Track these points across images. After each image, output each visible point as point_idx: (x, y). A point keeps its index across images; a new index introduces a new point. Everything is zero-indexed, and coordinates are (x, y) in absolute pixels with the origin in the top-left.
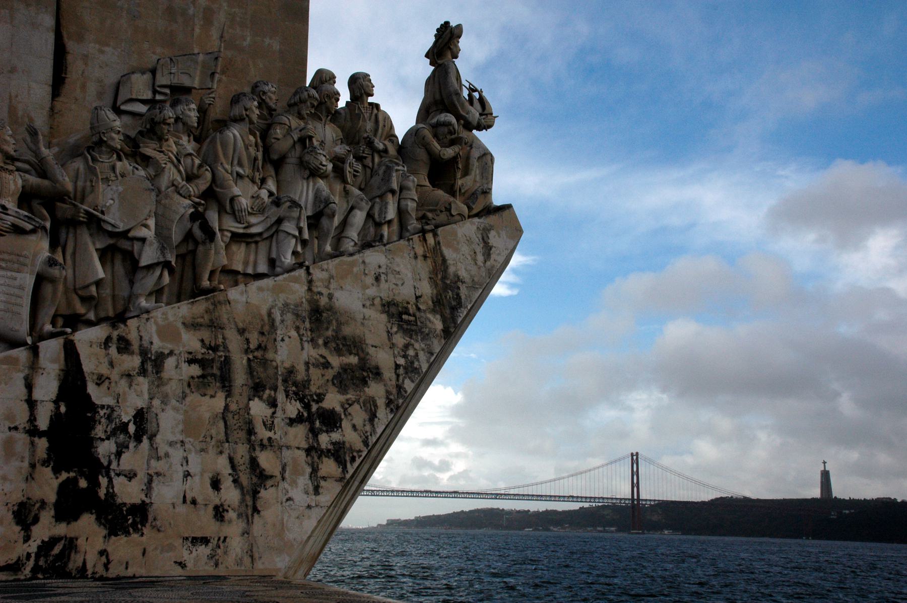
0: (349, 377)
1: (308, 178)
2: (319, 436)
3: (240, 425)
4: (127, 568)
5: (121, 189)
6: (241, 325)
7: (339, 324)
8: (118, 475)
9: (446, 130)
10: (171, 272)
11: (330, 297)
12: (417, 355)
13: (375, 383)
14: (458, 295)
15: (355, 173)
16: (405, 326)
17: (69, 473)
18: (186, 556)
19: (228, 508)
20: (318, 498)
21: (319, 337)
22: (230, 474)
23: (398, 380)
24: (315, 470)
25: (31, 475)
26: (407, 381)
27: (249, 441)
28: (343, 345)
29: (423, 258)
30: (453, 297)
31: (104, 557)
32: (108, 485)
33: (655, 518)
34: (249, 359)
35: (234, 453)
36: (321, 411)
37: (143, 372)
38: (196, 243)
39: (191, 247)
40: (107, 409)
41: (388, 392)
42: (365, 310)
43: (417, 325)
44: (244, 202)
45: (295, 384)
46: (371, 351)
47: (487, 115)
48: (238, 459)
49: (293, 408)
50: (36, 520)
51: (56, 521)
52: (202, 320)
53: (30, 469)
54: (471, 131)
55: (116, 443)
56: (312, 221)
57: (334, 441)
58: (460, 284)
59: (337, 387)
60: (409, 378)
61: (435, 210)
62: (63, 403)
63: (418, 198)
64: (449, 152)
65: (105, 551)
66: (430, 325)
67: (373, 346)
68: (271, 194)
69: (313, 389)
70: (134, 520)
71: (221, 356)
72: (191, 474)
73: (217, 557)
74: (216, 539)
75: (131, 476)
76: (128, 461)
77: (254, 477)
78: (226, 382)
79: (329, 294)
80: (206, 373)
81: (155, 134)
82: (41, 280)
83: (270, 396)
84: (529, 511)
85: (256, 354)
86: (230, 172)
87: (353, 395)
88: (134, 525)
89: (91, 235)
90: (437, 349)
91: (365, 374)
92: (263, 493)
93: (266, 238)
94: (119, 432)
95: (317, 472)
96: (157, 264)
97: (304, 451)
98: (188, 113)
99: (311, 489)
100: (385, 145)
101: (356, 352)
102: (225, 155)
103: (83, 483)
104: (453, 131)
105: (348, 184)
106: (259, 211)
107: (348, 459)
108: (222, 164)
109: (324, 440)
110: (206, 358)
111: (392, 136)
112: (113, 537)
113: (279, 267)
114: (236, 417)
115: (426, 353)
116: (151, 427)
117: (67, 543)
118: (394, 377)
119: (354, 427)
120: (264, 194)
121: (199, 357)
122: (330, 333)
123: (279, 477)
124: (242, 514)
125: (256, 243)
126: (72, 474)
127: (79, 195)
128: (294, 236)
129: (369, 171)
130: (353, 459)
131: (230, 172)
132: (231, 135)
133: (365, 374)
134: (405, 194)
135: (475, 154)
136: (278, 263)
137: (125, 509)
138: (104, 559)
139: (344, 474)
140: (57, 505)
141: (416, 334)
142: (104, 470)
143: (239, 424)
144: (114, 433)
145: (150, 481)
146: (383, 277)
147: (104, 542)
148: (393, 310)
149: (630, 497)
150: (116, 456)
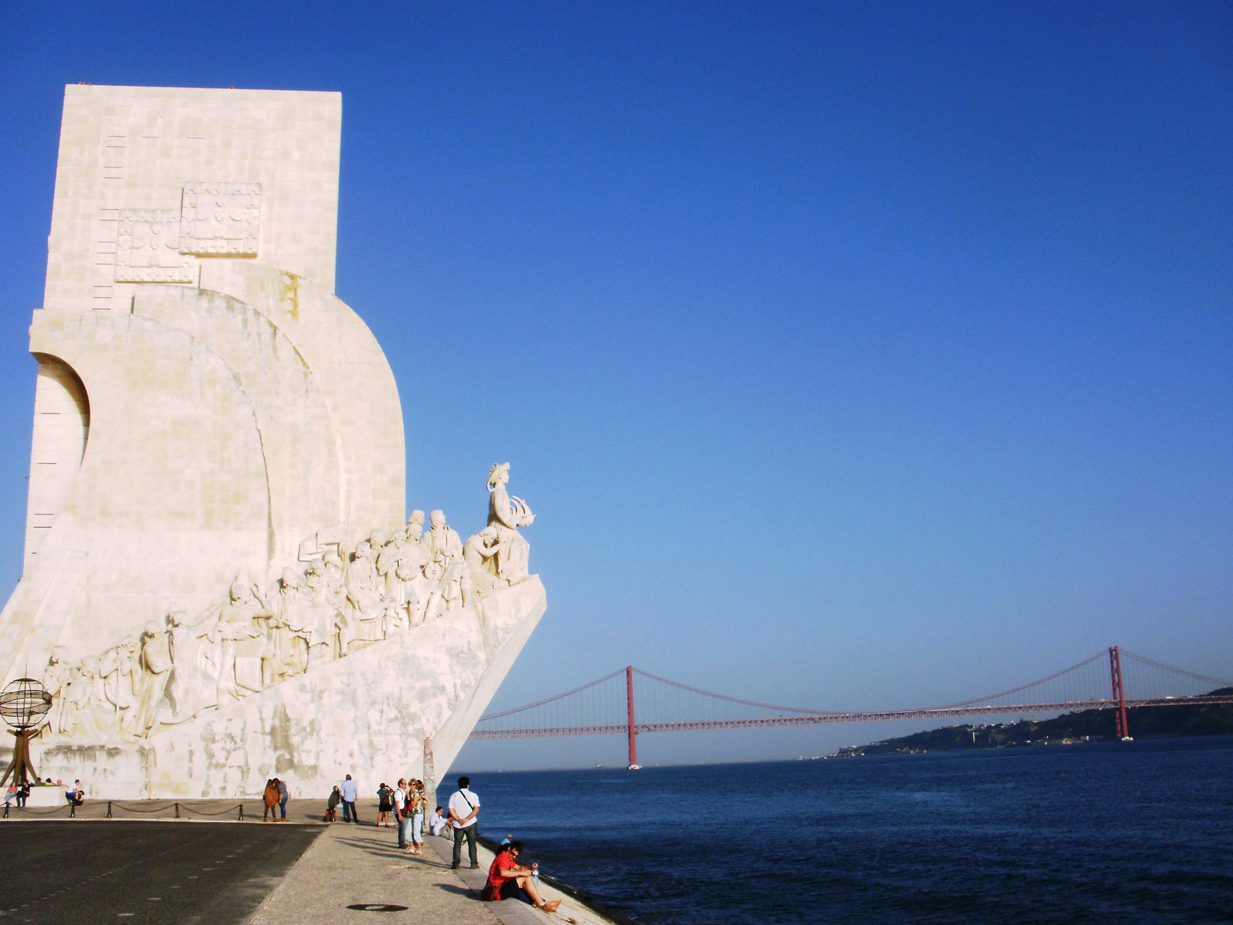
8: (303, 752)
24: (405, 745)
27: (368, 731)
34: (368, 689)
37: (312, 700)
41: (450, 699)
49: (392, 714)
75: (309, 752)
78: (354, 702)
90: (481, 672)
92: (376, 758)
103: (287, 756)
109: (410, 729)
119: (428, 720)
138: (298, 791)
145: (318, 754)
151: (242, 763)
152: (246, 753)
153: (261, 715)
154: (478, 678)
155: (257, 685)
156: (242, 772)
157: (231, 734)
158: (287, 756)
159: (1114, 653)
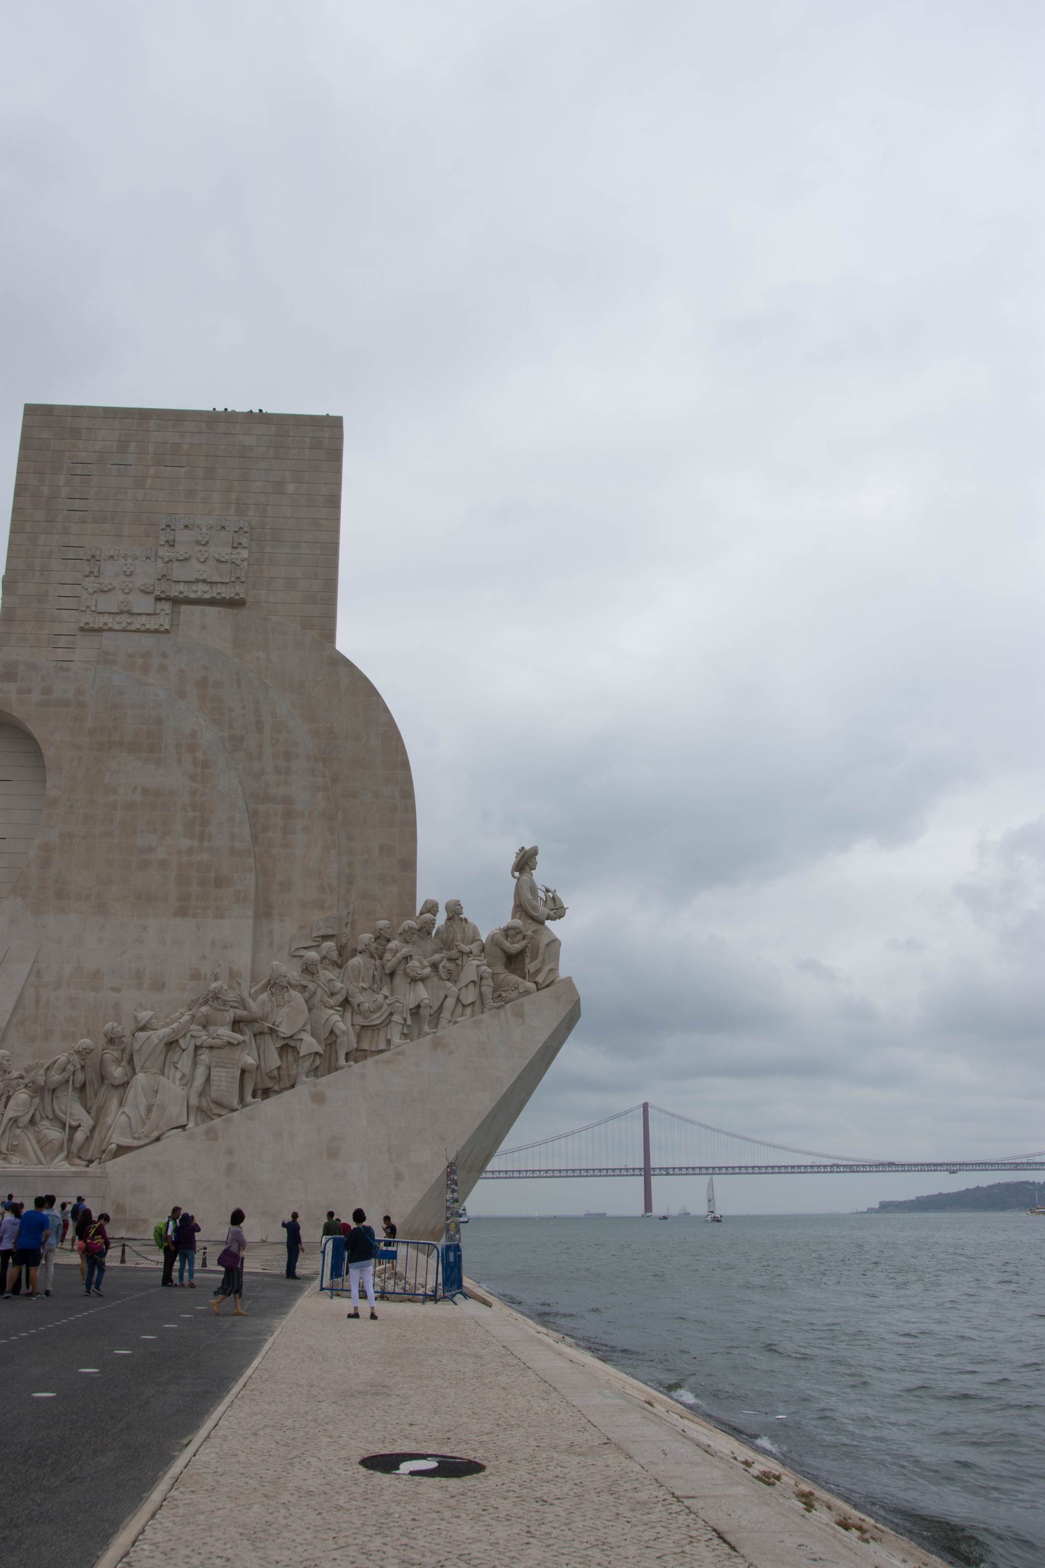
1: (410, 983)
5: (288, 1010)
38: (337, 1037)
39: (334, 1039)
61: (508, 990)
64: (515, 947)
82: (243, 1071)
89: (273, 1039)
96: (311, 1053)
105: (443, 980)
111: (475, 939)
120: (380, 997)
125: (379, 1029)
129: (460, 968)
134: (484, 982)
135: (545, 940)
155: (235, 1102)
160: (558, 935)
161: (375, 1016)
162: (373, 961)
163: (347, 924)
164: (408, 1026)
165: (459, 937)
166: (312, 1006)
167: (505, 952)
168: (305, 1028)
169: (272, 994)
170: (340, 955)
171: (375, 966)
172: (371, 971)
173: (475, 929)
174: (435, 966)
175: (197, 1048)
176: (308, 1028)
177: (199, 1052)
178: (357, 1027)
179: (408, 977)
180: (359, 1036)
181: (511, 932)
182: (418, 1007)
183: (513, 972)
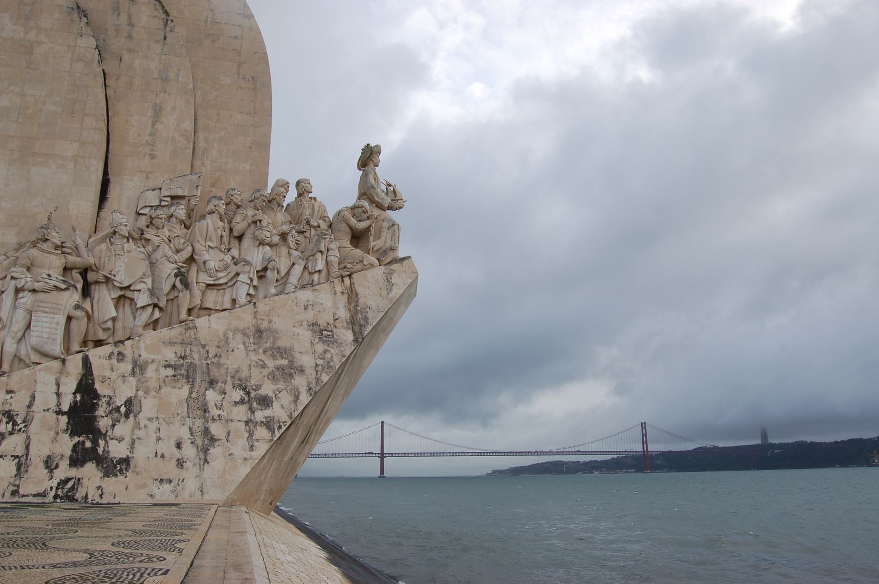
0: (280, 374)
2: (255, 413)
3: (198, 406)
4: (114, 498)
5: (126, 260)
6: (203, 343)
7: (275, 339)
8: (112, 439)
9: (360, 210)
10: (161, 309)
11: (270, 322)
12: (332, 357)
13: (299, 376)
14: (366, 317)
15: (297, 242)
16: (324, 339)
17: (79, 438)
18: (155, 490)
19: (187, 460)
20: (252, 453)
21: (259, 348)
22: (189, 438)
23: (317, 374)
24: (251, 434)
25: (55, 439)
26: (324, 374)
28: (277, 353)
29: (341, 294)
30: (362, 318)
31: (100, 490)
32: (105, 445)
33: (659, 462)
35: (193, 425)
36: (258, 396)
37: (133, 374)
40: (107, 398)
41: (308, 382)
42: (295, 329)
43: (333, 338)
44: (212, 264)
45: (240, 380)
46: (298, 356)
47: (398, 200)
48: (195, 428)
49: (238, 395)
50: (57, 466)
51: (70, 467)
52: (177, 340)
53: (55, 435)
54: (385, 211)
55: (112, 419)
56: (260, 274)
57: (266, 416)
58: (368, 310)
59: (271, 380)
60: (325, 373)
61: (353, 262)
62: (78, 394)
63: (340, 255)
64: (362, 225)
65: (101, 486)
66: (343, 337)
67: (299, 353)
68: (234, 258)
69: (253, 382)
70: (121, 468)
71: (188, 362)
72: (162, 439)
73: (177, 492)
74: (177, 480)
76: (119, 430)
77: (206, 440)
79: (269, 320)
80: (176, 373)
81: (153, 225)
82: (69, 318)
83: (221, 387)
84: (579, 461)
85: (213, 360)
86: (204, 245)
87: (282, 385)
88: (121, 471)
89: (109, 290)
91: (292, 371)
92: (212, 450)
93: (231, 286)
94: (114, 412)
95: (252, 436)
96: (149, 305)
97: (244, 422)
98: (178, 211)
99: (248, 446)
100: (318, 223)
101: (286, 357)
102: (201, 235)
103: (88, 444)
104: (365, 210)
105: (292, 249)
106: (224, 269)
107: (276, 427)
108: (198, 241)
109: (260, 415)
110: (177, 364)
111: (324, 218)
112: (106, 478)
113: (238, 304)
114: (196, 401)
115: (339, 356)
116: (135, 408)
117: (76, 481)
118: (314, 373)
119: (282, 405)
120: (228, 259)
121: (173, 363)
122: (268, 345)
123: (225, 440)
124: (196, 464)
125: (224, 289)
126: (82, 439)
127: (101, 267)
128: (247, 284)
129: (308, 240)
130: (280, 427)
131: (204, 245)
132: (206, 223)
133: (292, 371)
134: (330, 253)
136: (237, 302)
137: (115, 460)
139: (273, 437)
140: (71, 458)
141: (333, 344)
142: (102, 436)
143: (198, 406)
144: (111, 412)
146: (310, 307)
147: (101, 481)
148: (315, 328)
149: (642, 450)
150: (111, 427)
151: (20, 451)
152: (28, 438)
153: (58, 389)
154: (344, 359)
155: (57, 349)
156: (19, 466)
157: (10, 411)
158: (88, 444)
159: (643, 425)
160: (397, 221)
161: (220, 275)
162: (221, 223)
163: (198, 186)
164: (255, 287)
165: (308, 212)
166: (154, 261)
167: (351, 228)
168: (145, 280)
169: (112, 243)
170: (190, 217)
171: (224, 228)
172: (219, 232)
173: (322, 206)
174: (284, 236)
175: (18, 291)
176: (149, 281)
177: (21, 295)
178: (201, 284)
179: (257, 240)
180: (203, 293)
181: (356, 211)
182: (265, 269)
183: (357, 248)
